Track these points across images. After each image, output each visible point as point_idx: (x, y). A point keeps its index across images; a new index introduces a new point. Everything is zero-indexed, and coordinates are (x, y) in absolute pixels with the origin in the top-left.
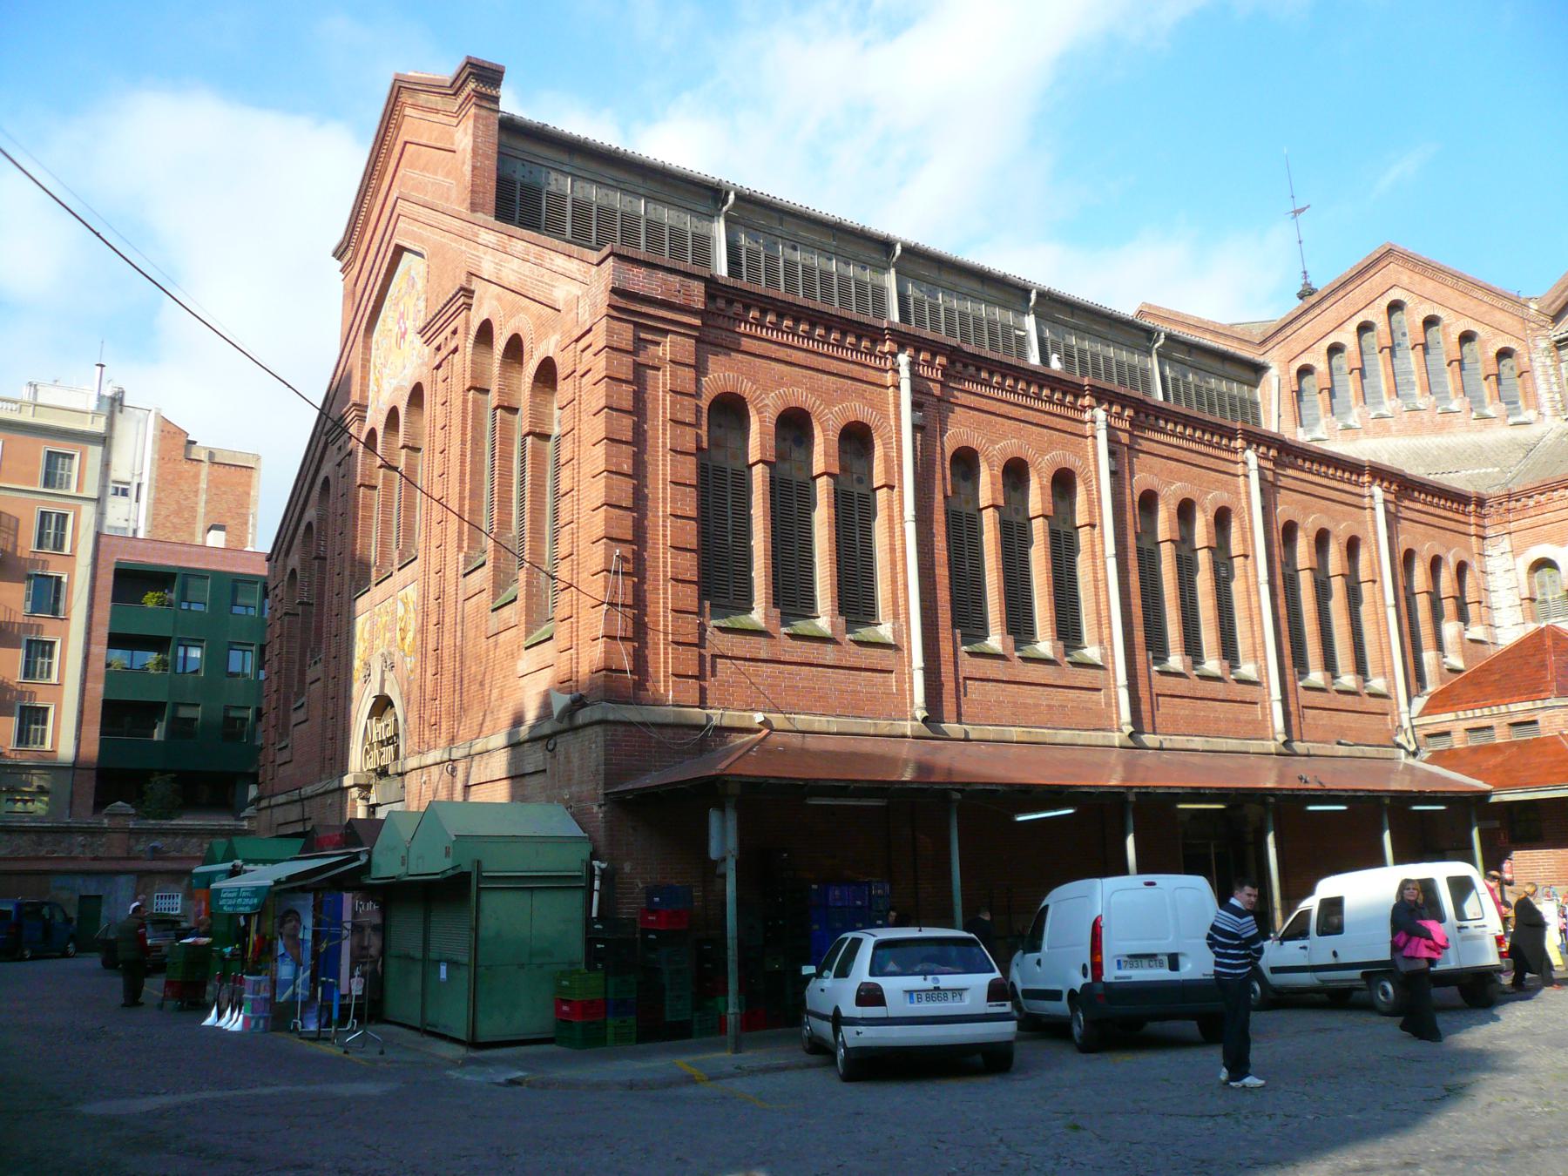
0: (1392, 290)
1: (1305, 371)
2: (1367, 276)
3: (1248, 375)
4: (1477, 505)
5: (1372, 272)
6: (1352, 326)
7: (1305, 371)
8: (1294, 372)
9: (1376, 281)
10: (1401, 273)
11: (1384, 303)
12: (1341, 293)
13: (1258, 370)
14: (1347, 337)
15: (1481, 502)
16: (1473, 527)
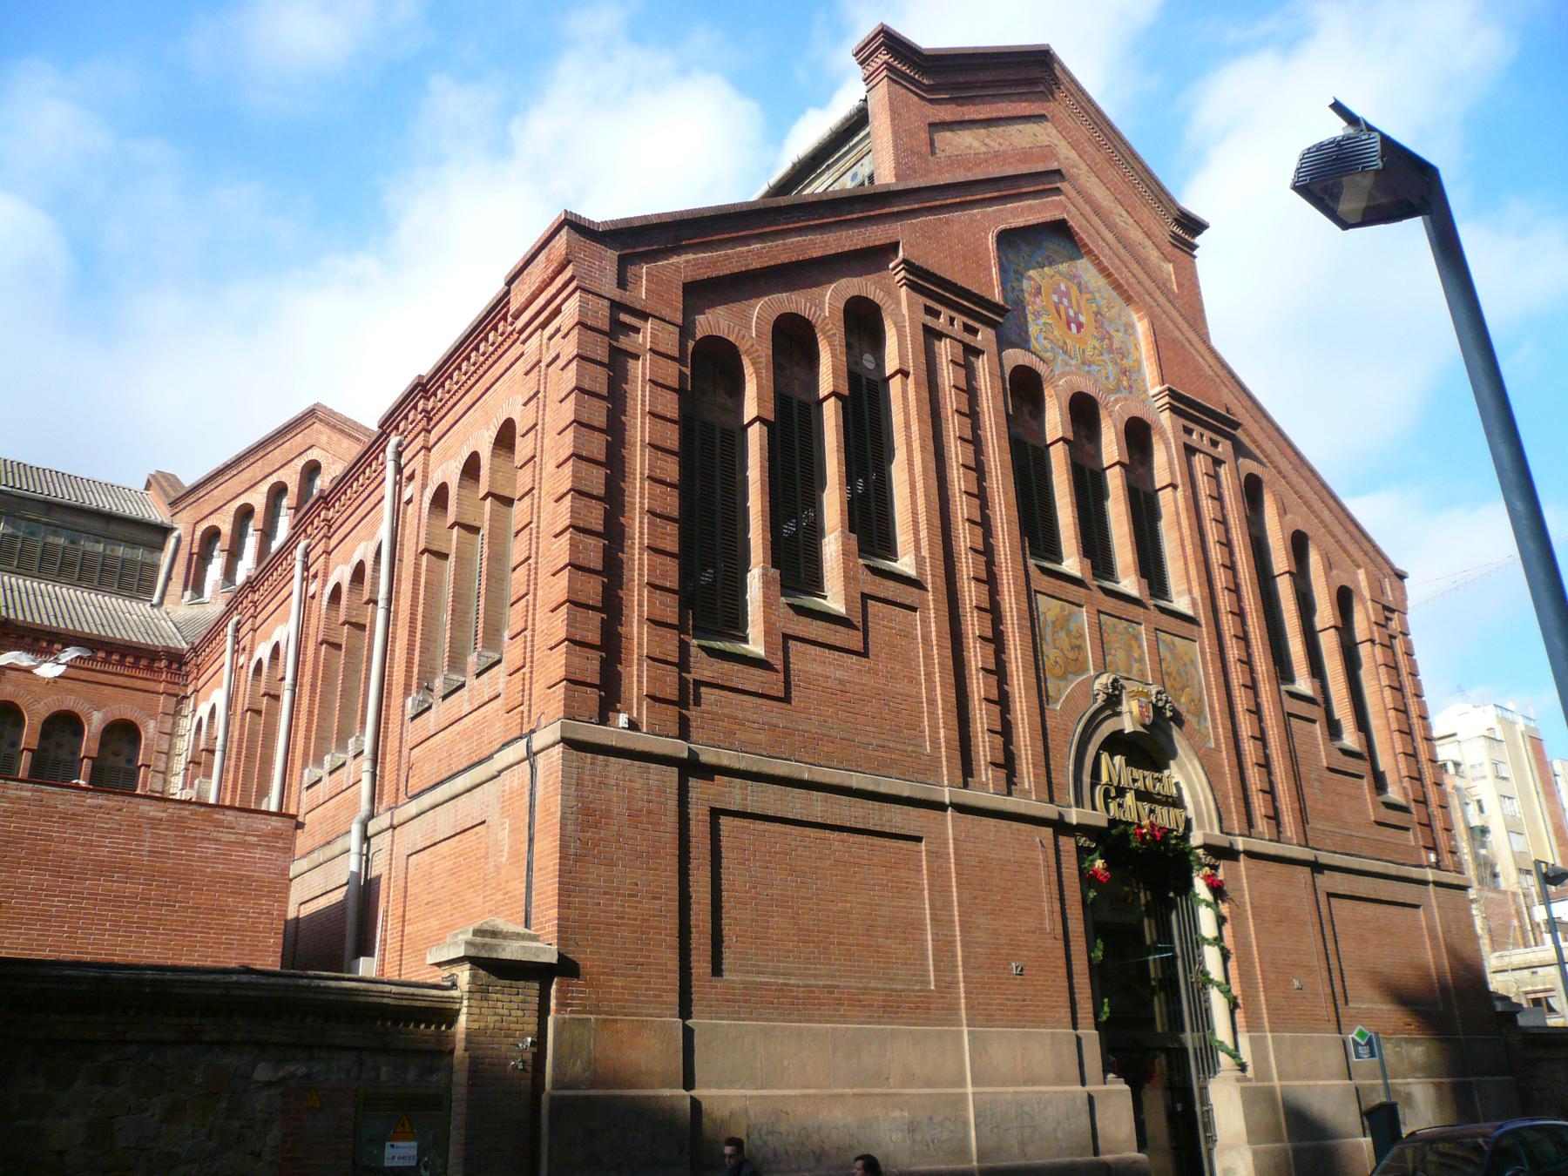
0: (310, 451)
1: (213, 535)
2: (288, 437)
3: (157, 538)
4: (171, 663)
5: (295, 432)
6: (264, 487)
7: (213, 535)
8: (198, 534)
9: (298, 441)
10: (321, 433)
11: (300, 463)
12: (262, 454)
13: (165, 531)
14: (258, 499)
15: (176, 660)
16: (162, 685)
